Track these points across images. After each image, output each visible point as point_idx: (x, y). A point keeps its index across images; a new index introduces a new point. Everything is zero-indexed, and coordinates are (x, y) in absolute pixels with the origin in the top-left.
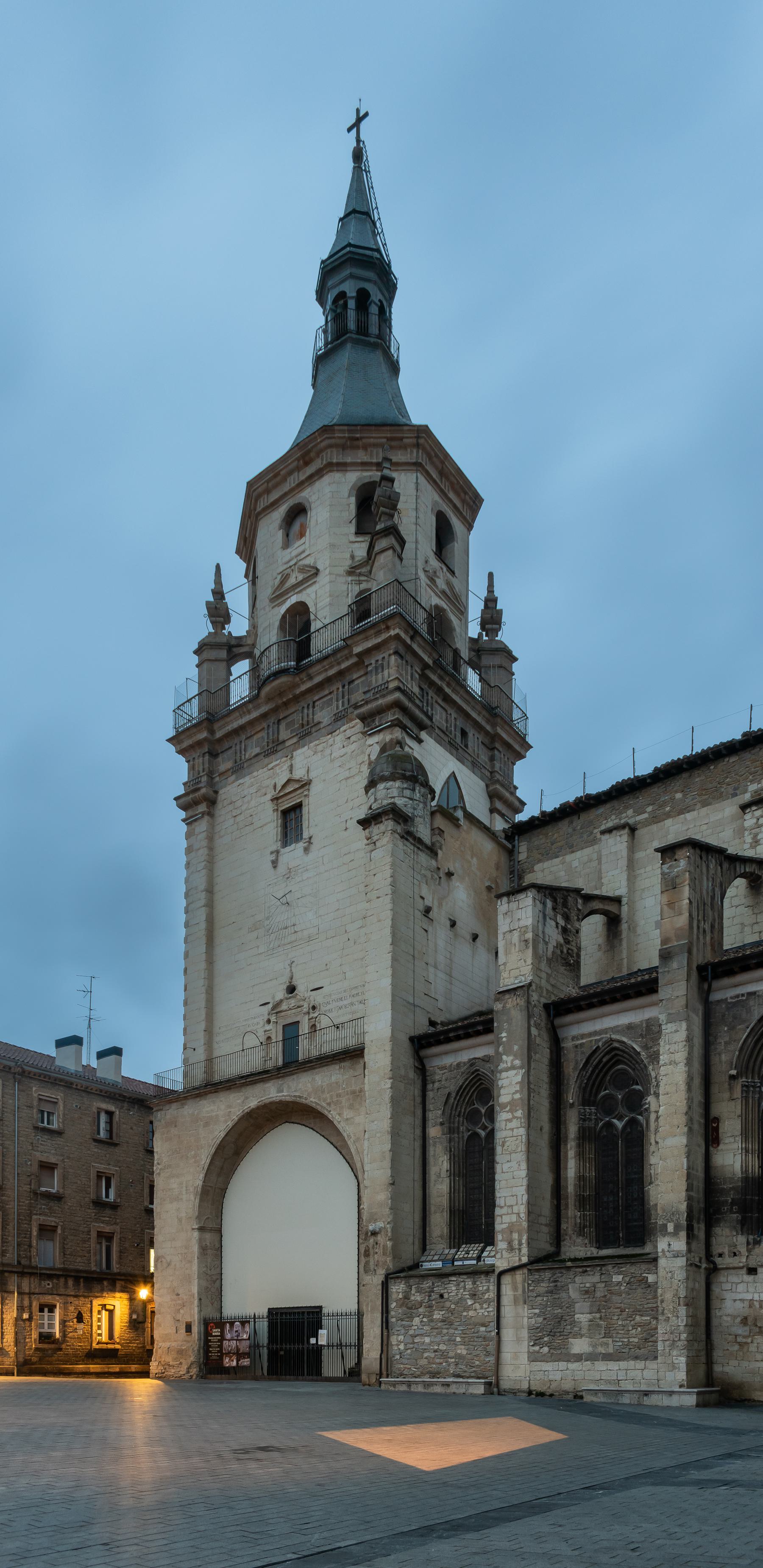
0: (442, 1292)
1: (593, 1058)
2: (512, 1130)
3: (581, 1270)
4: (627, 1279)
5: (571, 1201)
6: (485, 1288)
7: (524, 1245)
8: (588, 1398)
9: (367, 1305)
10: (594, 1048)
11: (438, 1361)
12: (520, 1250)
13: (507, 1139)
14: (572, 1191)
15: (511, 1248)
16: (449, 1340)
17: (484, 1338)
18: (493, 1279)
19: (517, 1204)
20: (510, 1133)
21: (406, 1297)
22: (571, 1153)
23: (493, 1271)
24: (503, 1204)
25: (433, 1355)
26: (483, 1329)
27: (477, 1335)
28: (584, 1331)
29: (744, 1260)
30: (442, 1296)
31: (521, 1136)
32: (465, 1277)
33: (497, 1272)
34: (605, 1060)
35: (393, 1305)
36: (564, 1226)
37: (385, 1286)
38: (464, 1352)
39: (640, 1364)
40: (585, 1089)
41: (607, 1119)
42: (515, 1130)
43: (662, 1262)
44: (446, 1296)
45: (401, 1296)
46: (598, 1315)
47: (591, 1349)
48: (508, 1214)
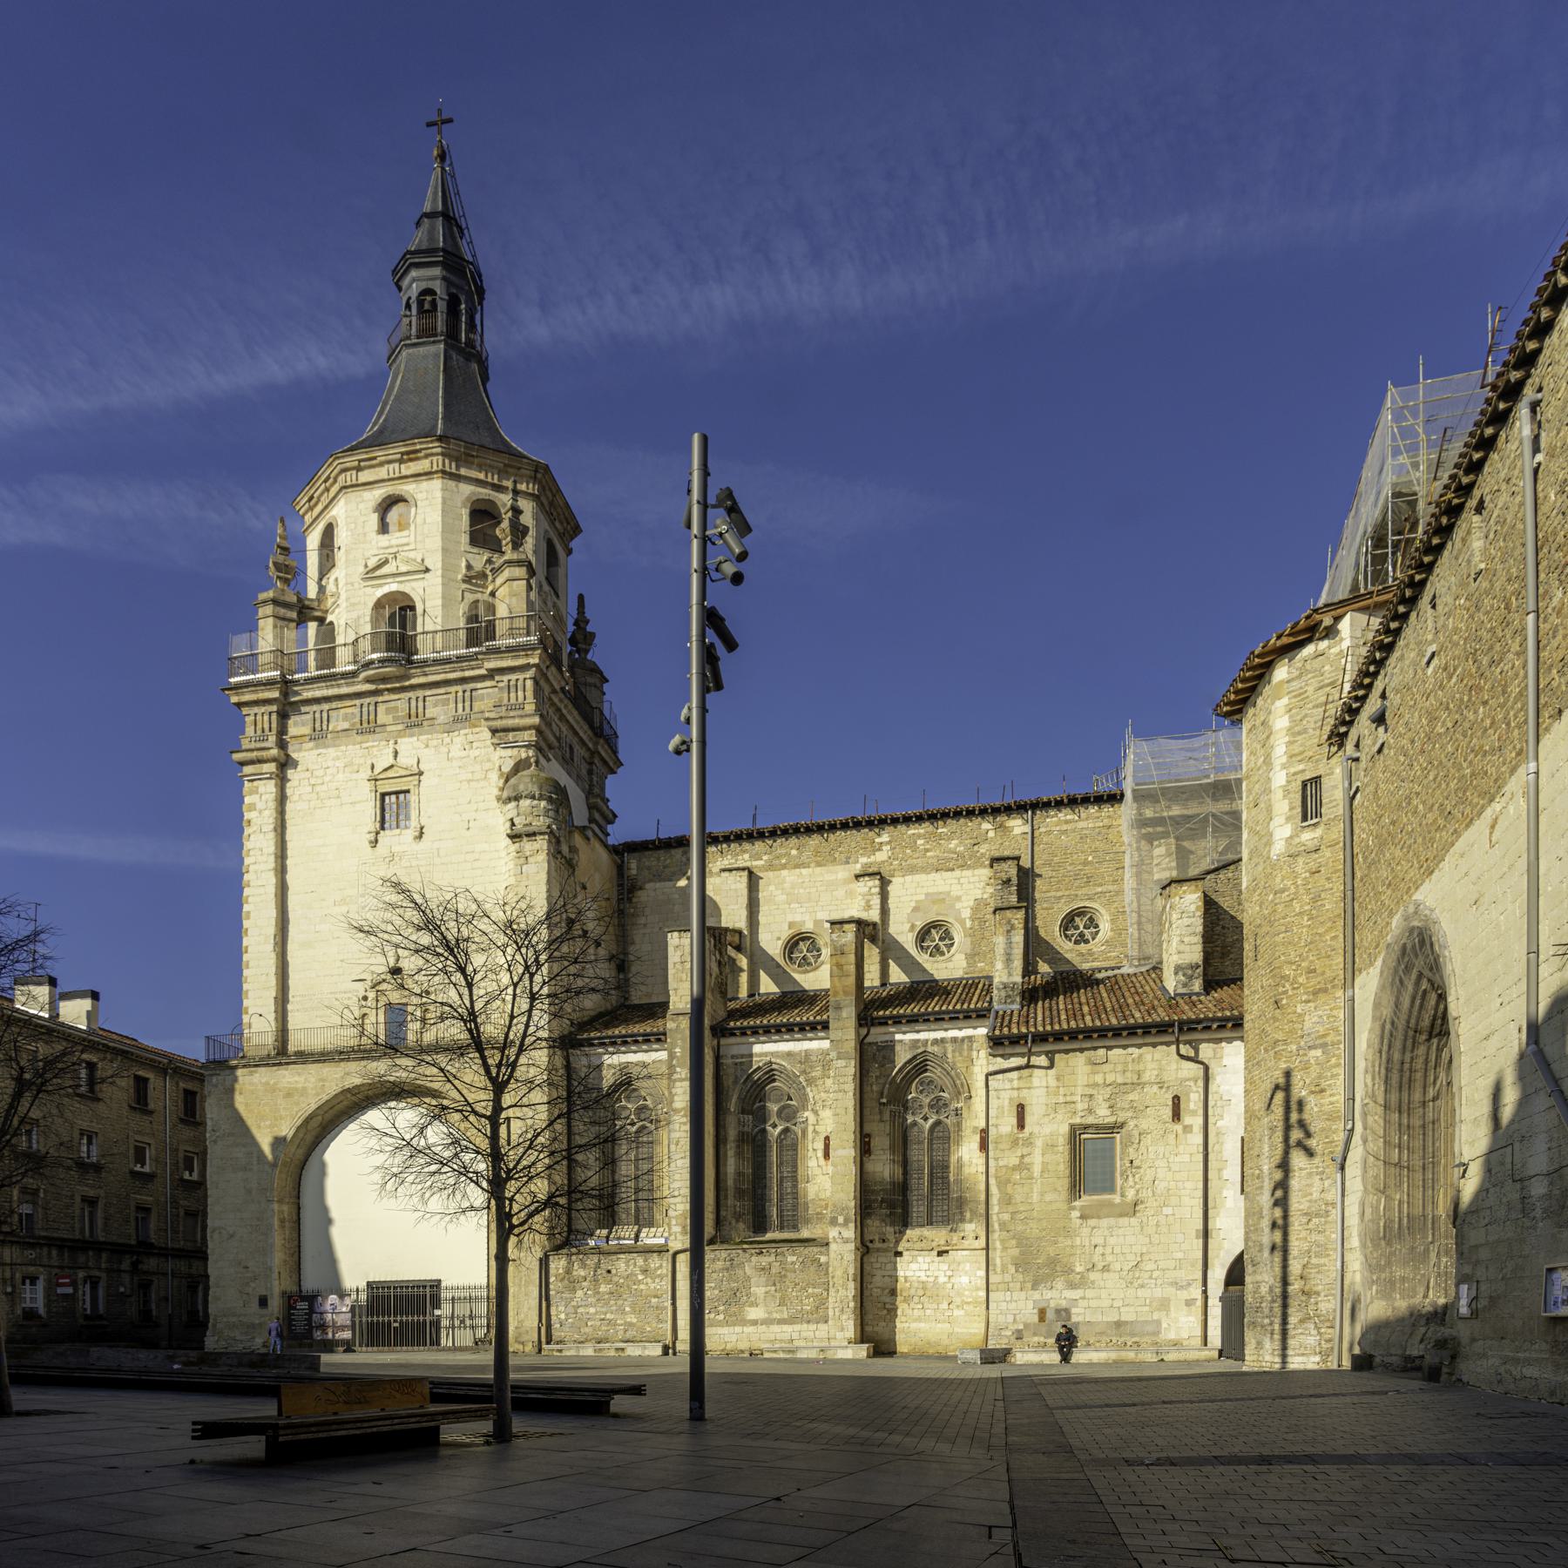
8: (766, 1355)
21: (568, 1271)
22: (731, 1153)
30: (609, 1272)
33: (671, 1252)
35: (552, 1279)
37: (544, 1263)
38: (635, 1321)
39: (813, 1327)
43: (833, 1246)
44: (614, 1271)
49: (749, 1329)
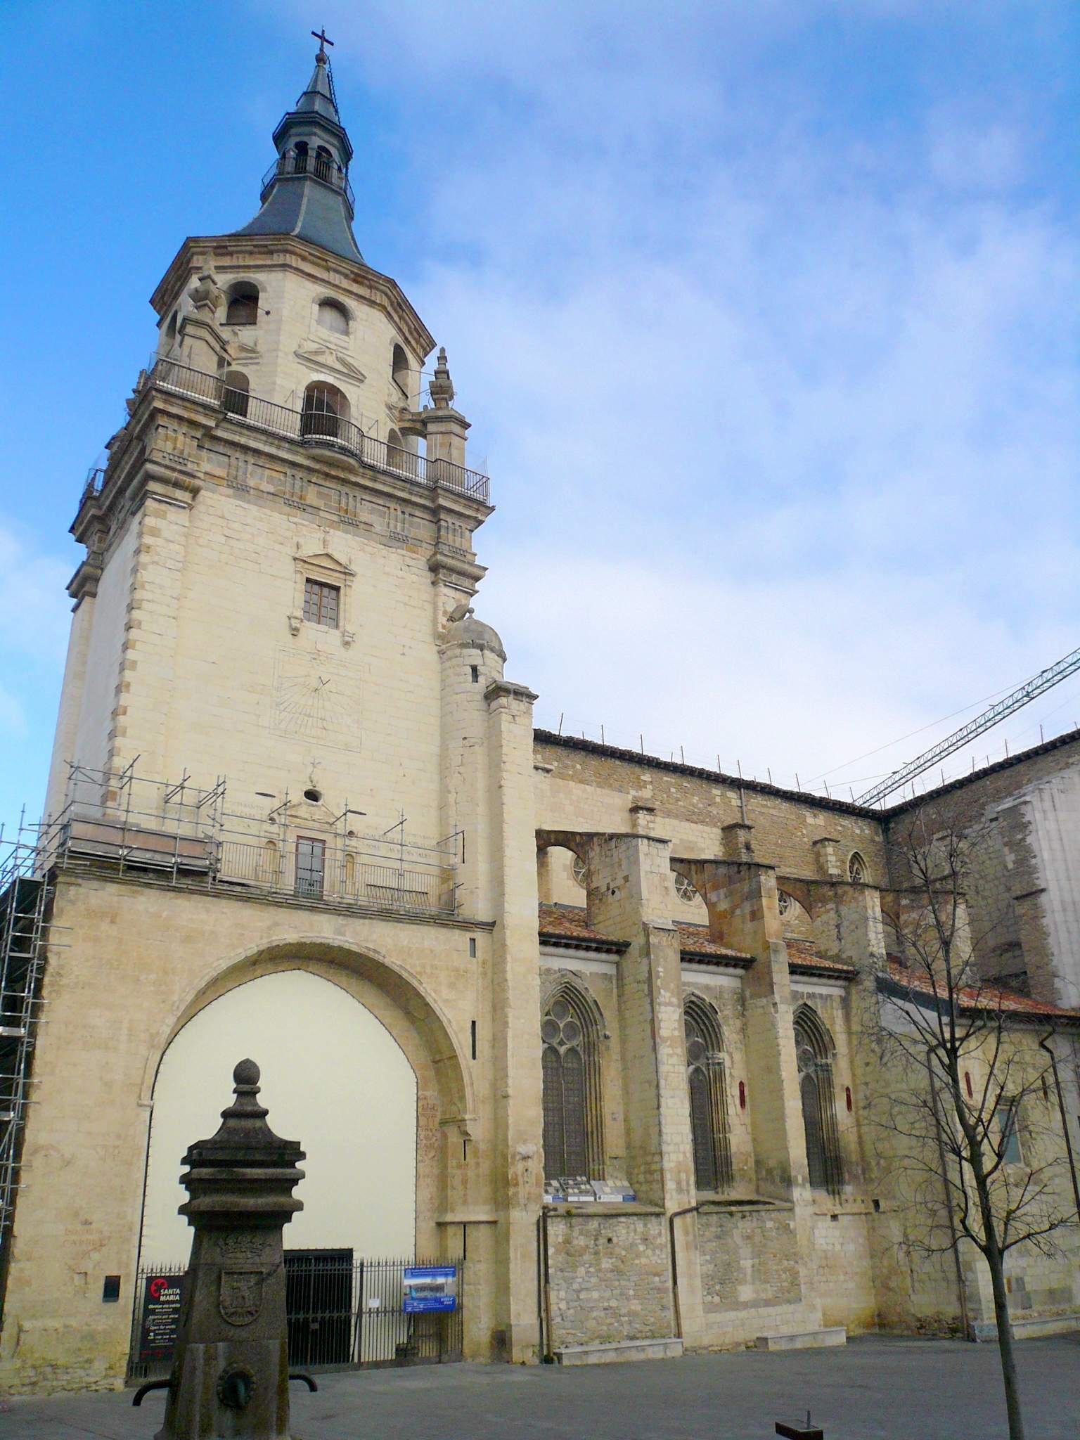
0: (610, 1235)
4: (777, 1225)
6: (657, 1232)
9: (516, 1250)
11: (609, 1321)
12: (688, 1192)
15: (680, 1190)
16: (621, 1294)
17: (659, 1289)
18: (664, 1221)
21: (567, 1241)
23: (663, 1214)
25: (602, 1314)
26: (657, 1279)
27: (651, 1286)
28: (749, 1278)
30: (610, 1240)
32: (635, 1218)
33: (669, 1214)
35: (551, 1251)
38: (639, 1308)
43: (797, 1210)
44: (615, 1240)
45: (560, 1239)
46: (757, 1261)
47: (755, 1295)
48: (675, 1152)
49: (743, 1314)
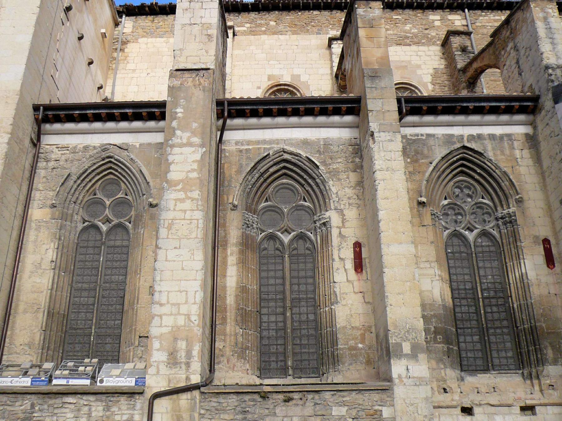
1: (261, 165)
2: (185, 211)
3: (281, 396)
5: (231, 315)
7: (196, 359)
10: (266, 154)
12: (188, 365)
13: (175, 222)
14: (233, 303)
19: (186, 302)
20: (180, 215)
24: (164, 300)
29: (456, 397)
31: (198, 220)
34: (271, 170)
36: (219, 345)
40: (249, 194)
41: (271, 231)
42: (188, 212)
48: (171, 314)
